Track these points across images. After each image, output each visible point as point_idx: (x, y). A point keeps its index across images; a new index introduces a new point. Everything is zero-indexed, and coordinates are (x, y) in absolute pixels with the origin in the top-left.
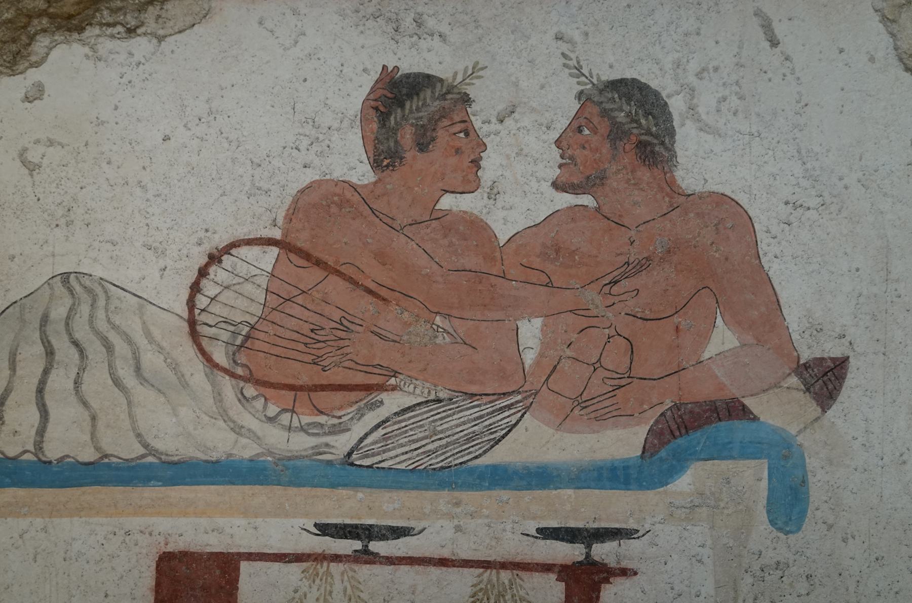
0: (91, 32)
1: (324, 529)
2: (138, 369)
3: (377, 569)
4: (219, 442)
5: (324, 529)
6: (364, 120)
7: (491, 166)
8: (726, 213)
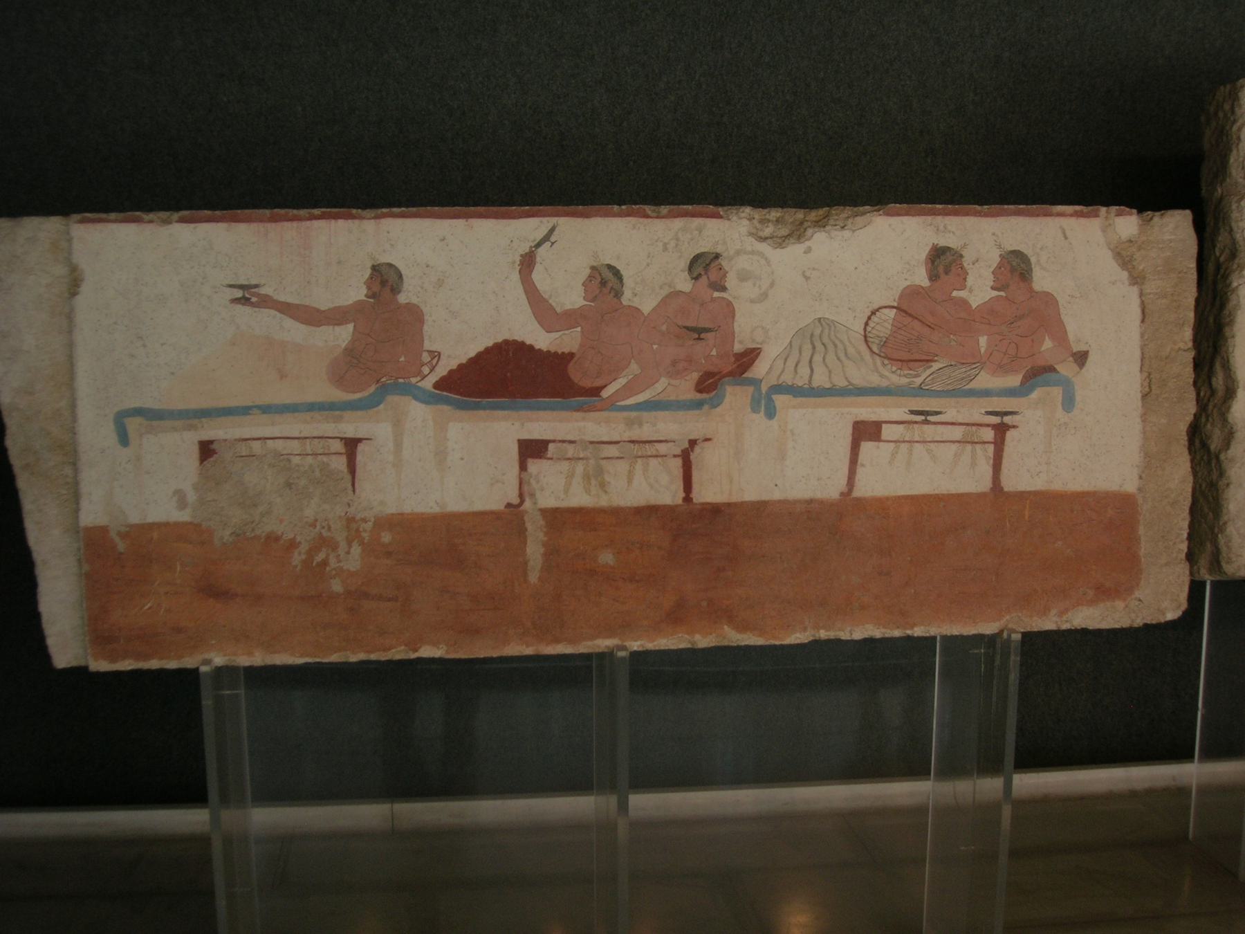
0: (828, 228)
1: (912, 412)
2: (846, 354)
3: (932, 427)
4: (875, 380)
5: (912, 412)
6: (926, 264)
7: (970, 281)
8: (1049, 300)
